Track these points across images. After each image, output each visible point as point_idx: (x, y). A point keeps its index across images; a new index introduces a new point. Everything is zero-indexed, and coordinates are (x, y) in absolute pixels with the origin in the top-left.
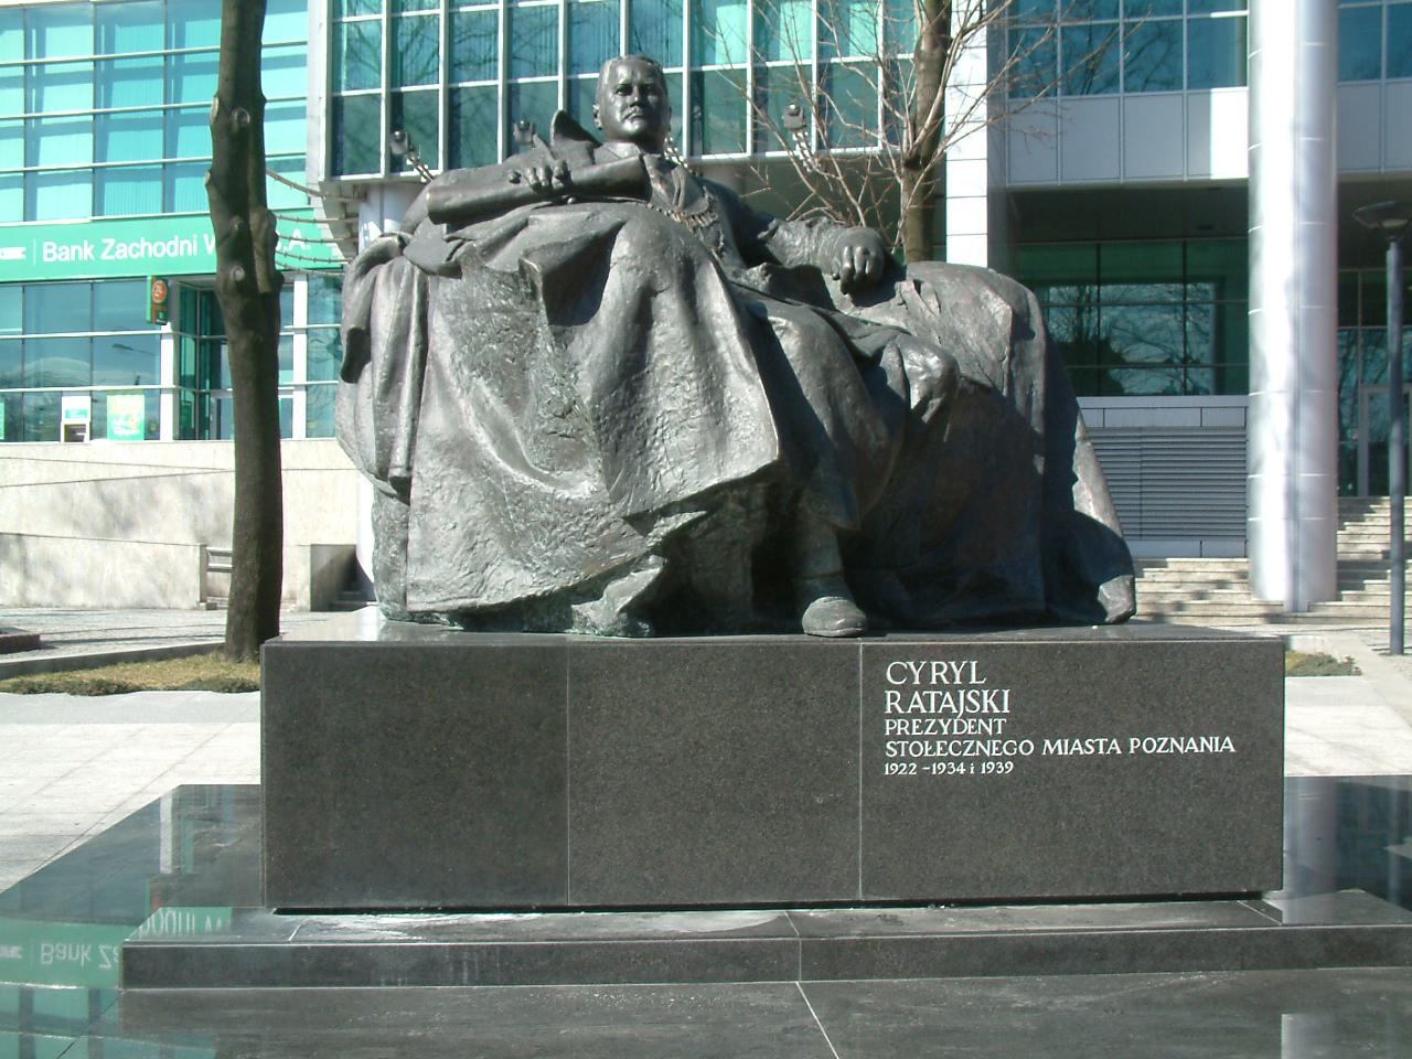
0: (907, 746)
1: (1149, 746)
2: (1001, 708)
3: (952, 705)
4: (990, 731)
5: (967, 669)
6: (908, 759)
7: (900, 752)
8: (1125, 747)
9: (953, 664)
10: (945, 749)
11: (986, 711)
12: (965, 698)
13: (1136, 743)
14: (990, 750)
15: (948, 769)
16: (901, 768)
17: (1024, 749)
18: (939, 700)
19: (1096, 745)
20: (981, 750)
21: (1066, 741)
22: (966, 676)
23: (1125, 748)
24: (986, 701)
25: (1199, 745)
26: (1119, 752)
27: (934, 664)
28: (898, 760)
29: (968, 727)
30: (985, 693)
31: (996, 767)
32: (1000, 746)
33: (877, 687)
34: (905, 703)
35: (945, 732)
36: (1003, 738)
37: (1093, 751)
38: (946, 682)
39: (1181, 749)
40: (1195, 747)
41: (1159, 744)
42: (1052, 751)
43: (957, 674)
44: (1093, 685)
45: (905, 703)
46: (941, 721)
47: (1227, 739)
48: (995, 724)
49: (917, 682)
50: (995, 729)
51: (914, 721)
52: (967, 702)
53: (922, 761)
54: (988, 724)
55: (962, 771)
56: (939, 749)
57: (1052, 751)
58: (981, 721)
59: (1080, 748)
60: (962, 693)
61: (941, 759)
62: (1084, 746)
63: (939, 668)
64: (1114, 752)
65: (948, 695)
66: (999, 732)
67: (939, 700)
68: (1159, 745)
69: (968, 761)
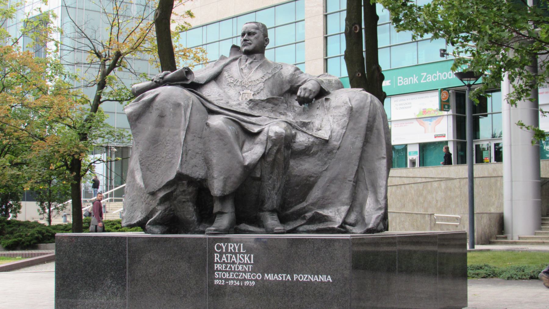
0: (221, 274)
1: (301, 278)
2: (250, 261)
3: (235, 260)
4: (247, 269)
5: (240, 246)
6: (222, 279)
7: (219, 276)
8: (292, 278)
9: (235, 244)
10: (233, 276)
11: (246, 262)
12: (239, 258)
13: (296, 276)
14: (247, 276)
15: (234, 283)
16: (219, 282)
17: (259, 276)
18: (231, 257)
19: (282, 277)
20: (244, 277)
21: (272, 275)
22: (239, 249)
23: (292, 278)
24: (246, 259)
25: (318, 278)
26: (290, 280)
27: (229, 244)
28: (218, 279)
29: (240, 268)
30: (246, 255)
31: (249, 283)
32: (250, 275)
33: (212, 252)
34: (220, 259)
35: (233, 270)
36: (251, 272)
37: (281, 279)
38: (233, 251)
39: (312, 280)
40: (317, 279)
41: (304, 277)
42: (267, 278)
43: (237, 248)
44: (281, 254)
45: (220, 259)
46: (232, 265)
47: (329, 276)
48: (249, 267)
49: (224, 251)
50: (249, 269)
51: (223, 265)
52: (240, 259)
53: (226, 280)
54: (246, 267)
55: (238, 284)
56: (231, 275)
57: (267, 278)
58: (244, 266)
59: (277, 278)
60: (238, 255)
61: (232, 279)
62: (278, 277)
63: (231, 246)
64: (288, 279)
65: (234, 256)
66: (250, 270)
67: (231, 257)
68: (304, 278)
69: (240, 280)
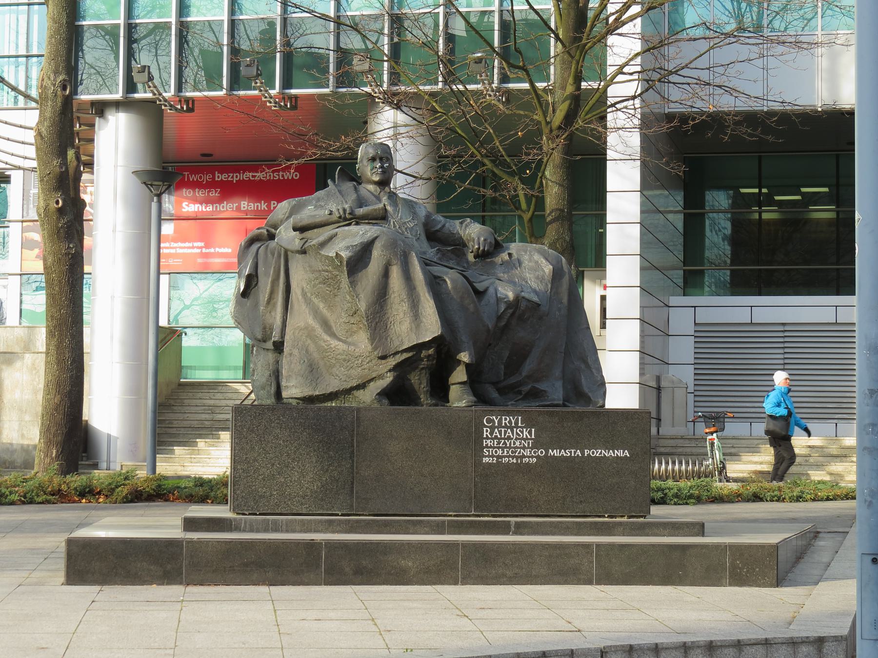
0: (492, 451)
1: (593, 453)
3: (511, 434)
4: (527, 446)
6: (493, 456)
11: (525, 437)
12: (516, 432)
13: (587, 452)
14: (527, 452)
16: (490, 460)
17: (541, 452)
18: (505, 432)
19: (571, 452)
20: (523, 453)
21: (558, 450)
25: (614, 453)
26: (580, 455)
27: (503, 417)
28: (489, 456)
29: (518, 444)
32: (530, 452)
34: (491, 433)
35: (508, 445)
41: (597, 452)
42: (552, 454)
43: (513, 421)
45: (491, 433)
46: (506, 441)
47: (626, 451)
48: (529, 443)
49: (496, 425)
50: (529, 445)
51: (495, 441)
52: (517, 433)
53: (498, 457)
55: (515, 462)
56: (506, 452)
57: (552, 454)
58: (523, 441)
60: (515, 429)
62: (566, 453)
63: (506, 419)
64: (578, 455)
65: (509, 430)
67: (505, 432)
68: (597, 453)
69: (517, 457)
